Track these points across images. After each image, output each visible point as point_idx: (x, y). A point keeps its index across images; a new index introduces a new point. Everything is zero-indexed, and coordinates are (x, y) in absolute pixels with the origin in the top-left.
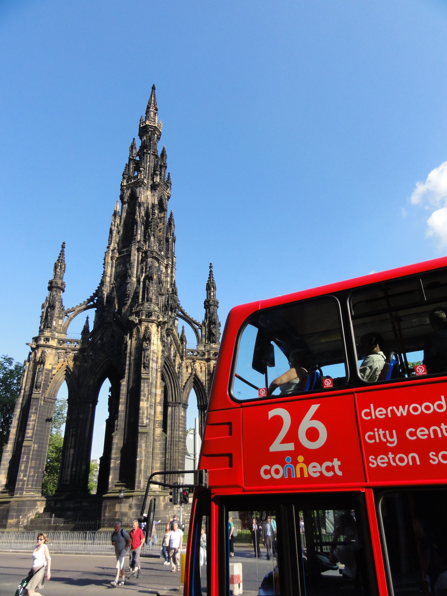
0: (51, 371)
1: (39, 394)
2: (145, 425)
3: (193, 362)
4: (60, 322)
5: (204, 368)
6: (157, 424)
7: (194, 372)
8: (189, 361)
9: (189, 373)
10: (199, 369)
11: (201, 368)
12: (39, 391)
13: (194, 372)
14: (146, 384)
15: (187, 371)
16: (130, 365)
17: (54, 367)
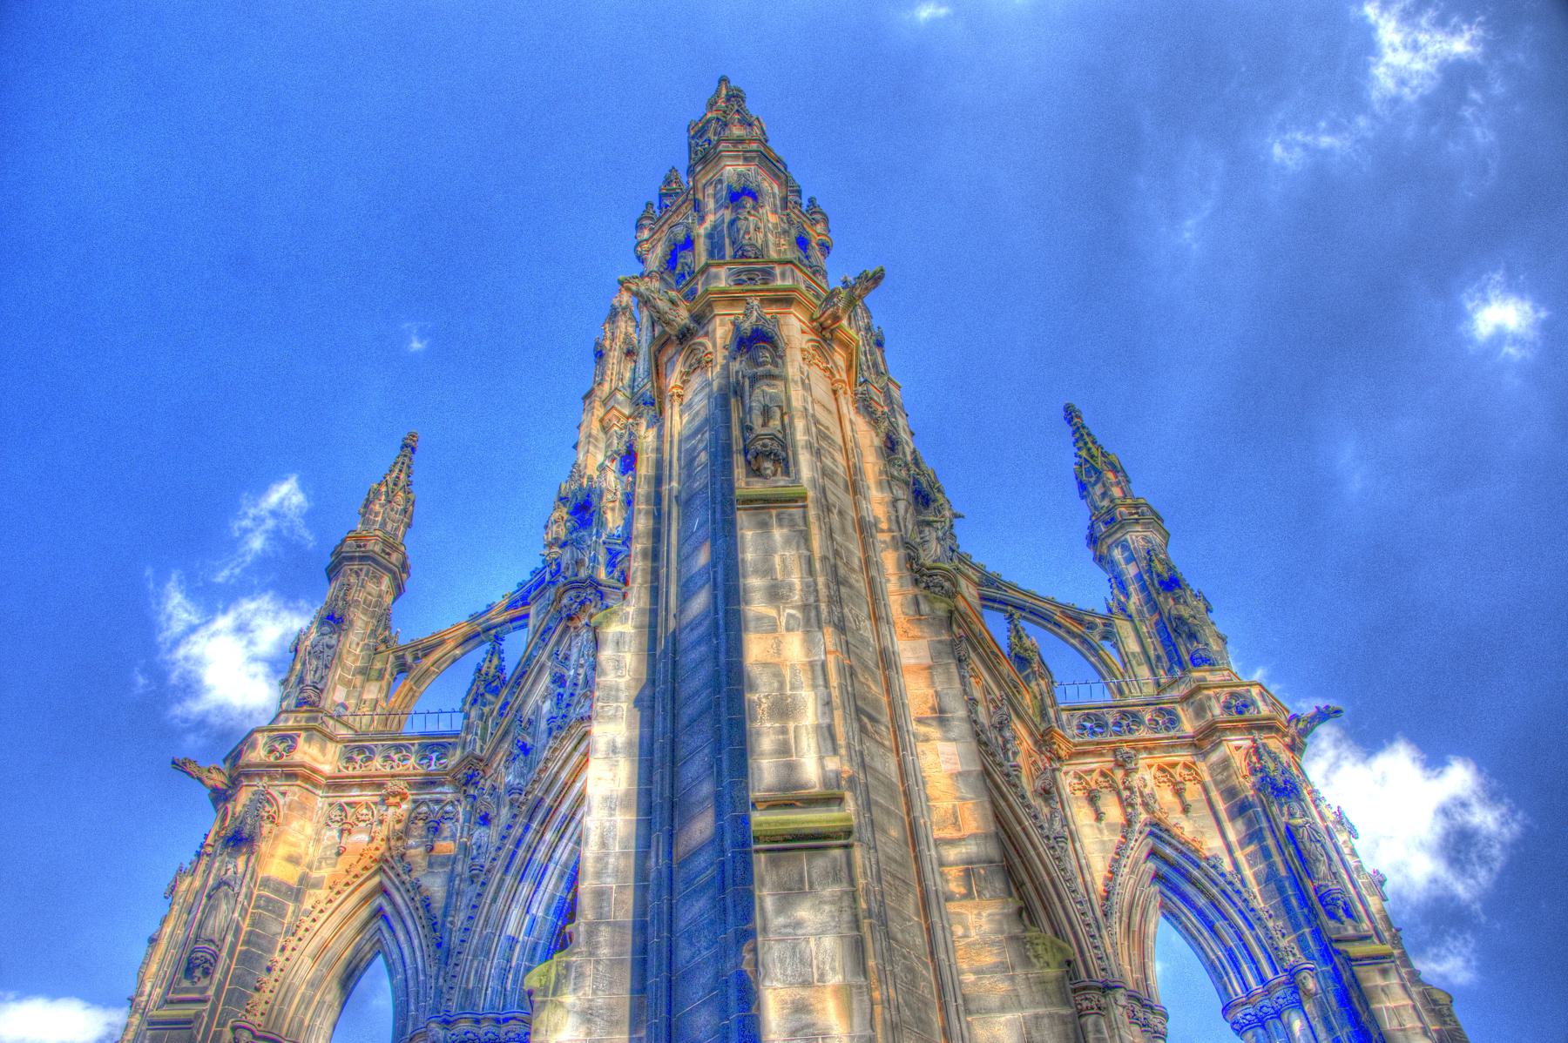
0: (297, 894)
1: (205, 1001)
2: (817, 789)
3: (1120, 765)
4: (372, 692)
5: (1192, 792)
6: (954, 872)
7: (1144, 816)
8: (1093, 763)
9: (1110, 826)
10: (1166, 796)
11: (1179, 793)
12: (206, 989)
13: (1144, 816)
14: (778, 534)
15: (1099, 817)
16: (656, 535)
17: (315, 874)
